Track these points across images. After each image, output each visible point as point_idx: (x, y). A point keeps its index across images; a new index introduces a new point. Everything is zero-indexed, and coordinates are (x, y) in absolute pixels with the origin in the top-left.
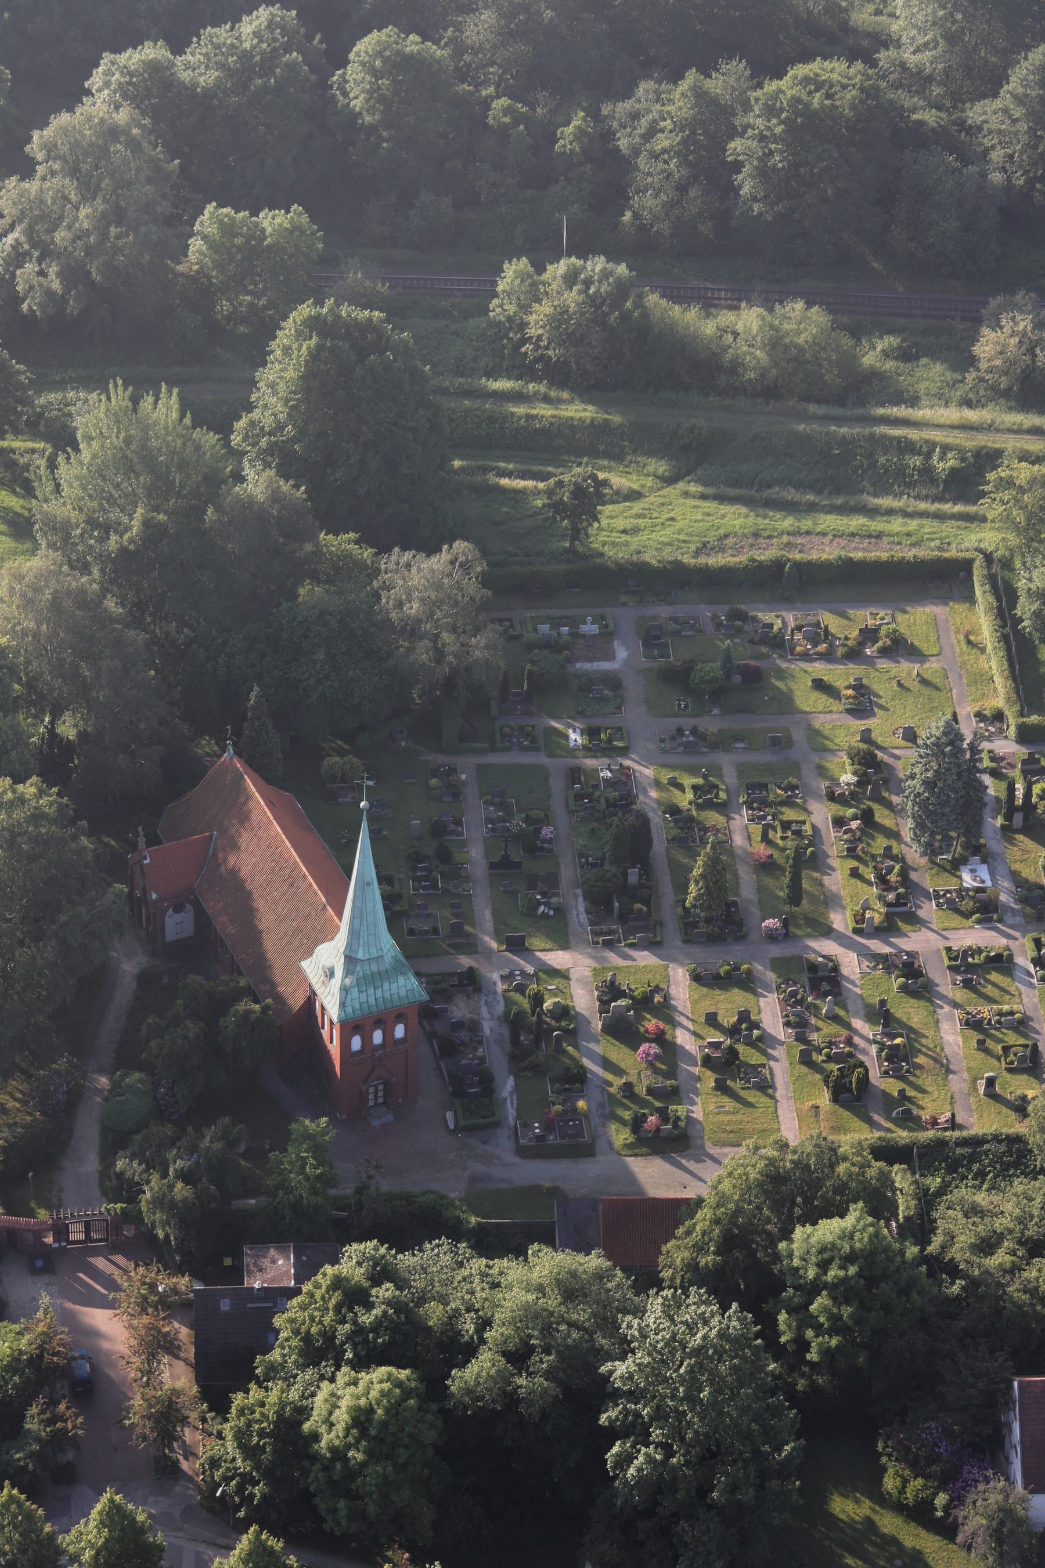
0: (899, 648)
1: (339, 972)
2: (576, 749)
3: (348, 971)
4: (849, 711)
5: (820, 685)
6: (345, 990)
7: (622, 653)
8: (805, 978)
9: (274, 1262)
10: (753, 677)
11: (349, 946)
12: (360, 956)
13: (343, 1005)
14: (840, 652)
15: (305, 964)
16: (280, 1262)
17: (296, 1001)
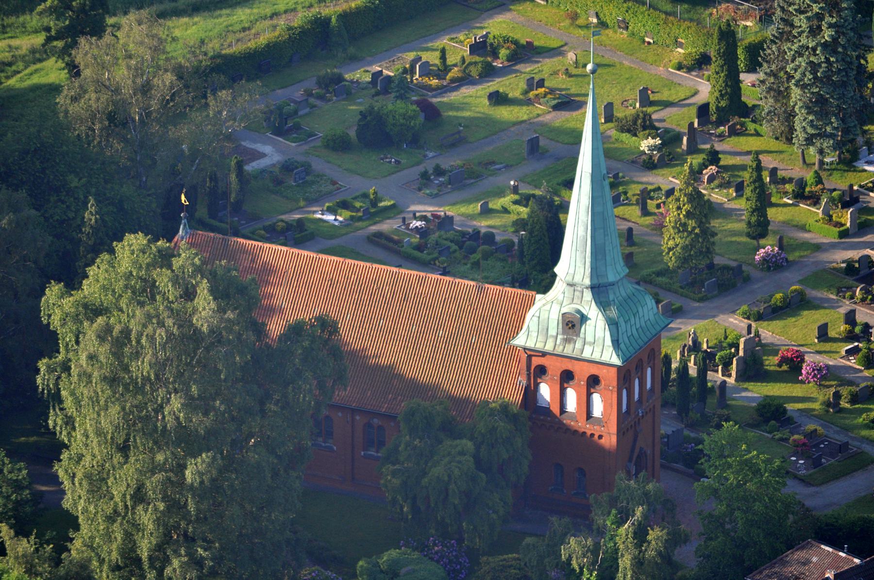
0: (524, 52)
1: (592, 311)
2: (344, 225)
3: (602, 302)
4: (556, 108)
5: (497, 98)
6: (612, 324)
7: (267, 149)
8: (850, 281)
9: (807, 562)
10: (432, 113)
11: (595, 271)
12: (611, 278)
13: (616, 343)
14: (474, 72)
15: (520, 340)
16: (815, 559)
17: (514, 395)
